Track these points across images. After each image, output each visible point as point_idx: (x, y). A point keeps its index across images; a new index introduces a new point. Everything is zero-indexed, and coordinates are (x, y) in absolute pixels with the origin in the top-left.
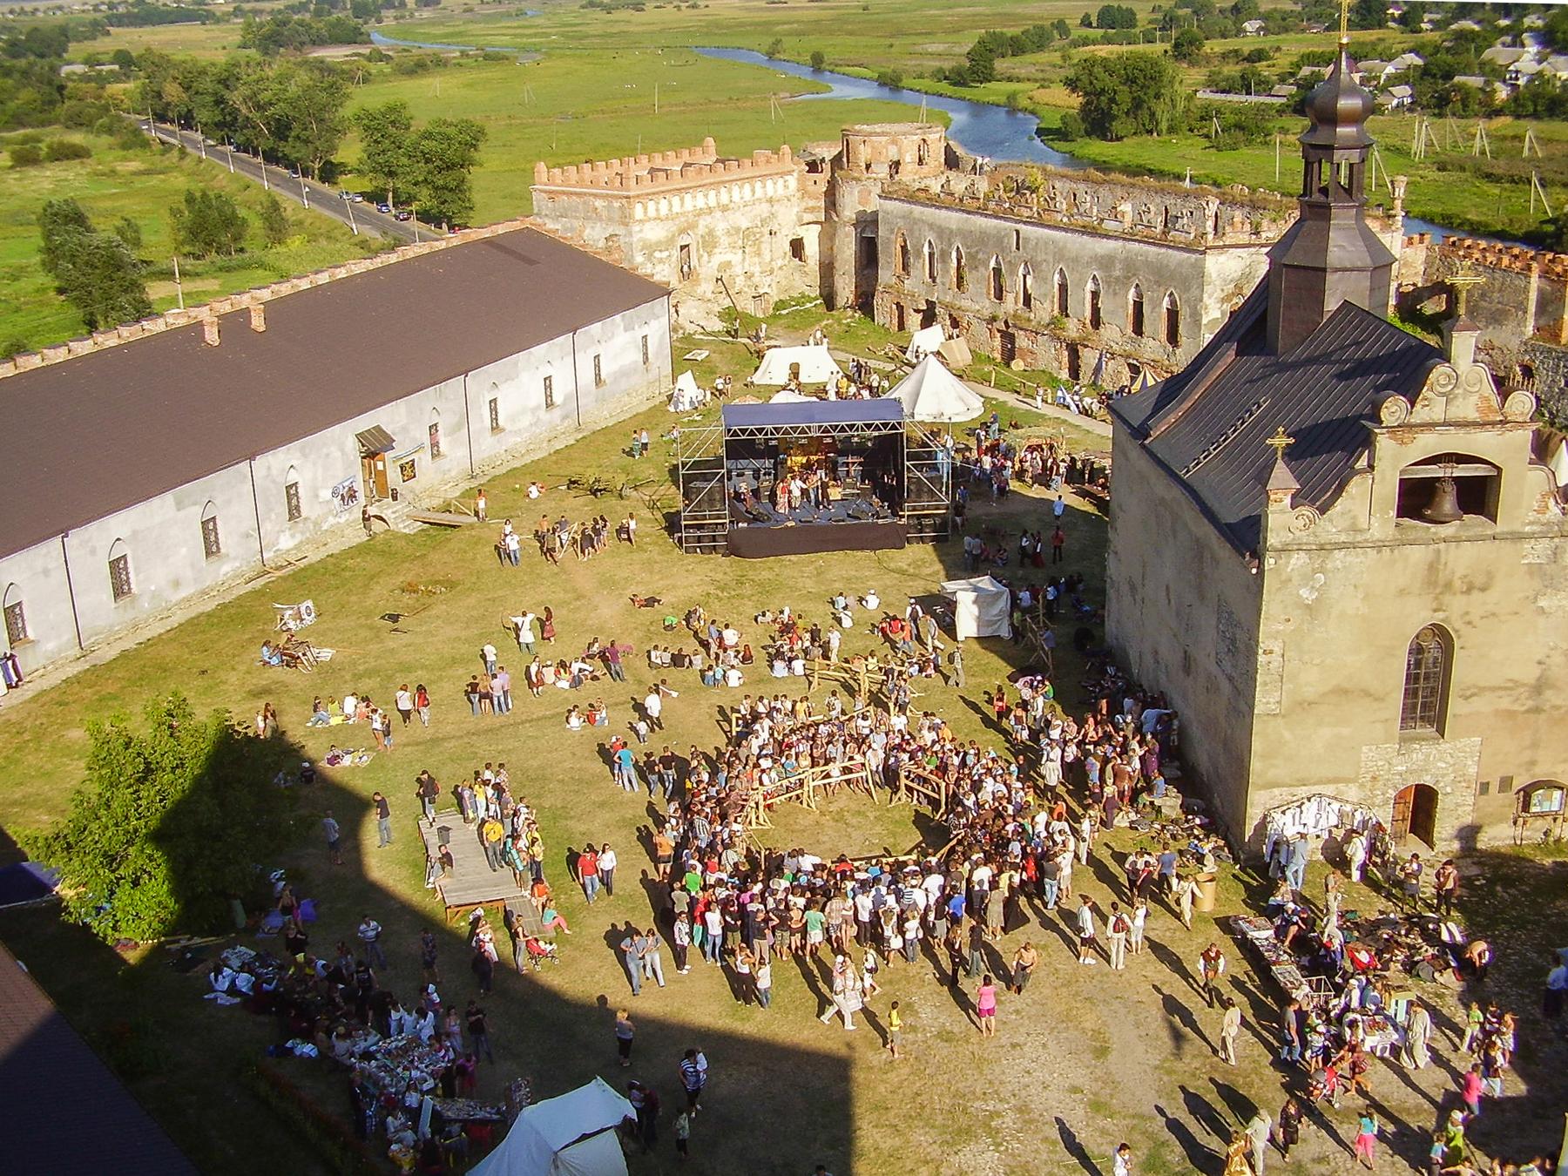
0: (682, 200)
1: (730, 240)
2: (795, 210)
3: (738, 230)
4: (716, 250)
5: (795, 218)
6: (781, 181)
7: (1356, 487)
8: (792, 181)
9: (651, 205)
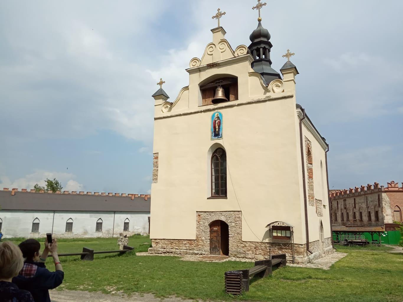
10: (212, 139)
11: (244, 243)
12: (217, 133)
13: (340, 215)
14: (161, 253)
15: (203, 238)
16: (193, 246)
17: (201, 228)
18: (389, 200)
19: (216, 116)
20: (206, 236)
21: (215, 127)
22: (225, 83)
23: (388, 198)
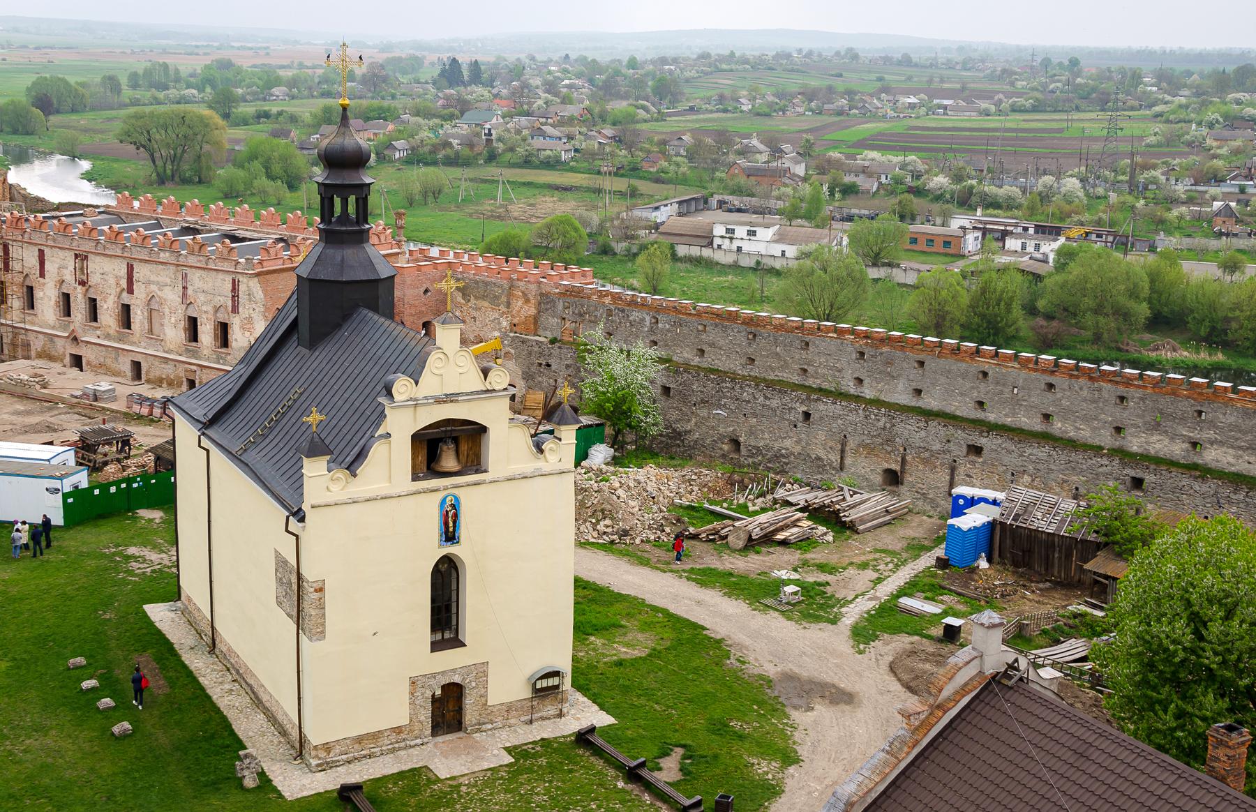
7: (377, 451)
10: (440, 546)
12: (450, 536)
13: (54, 299)
15: (423, 718)
16: (403, 736)
18: (262, 296)
19: (448, 503)
20: (425, 715)
21: (446, 524)
23: (260, 292)
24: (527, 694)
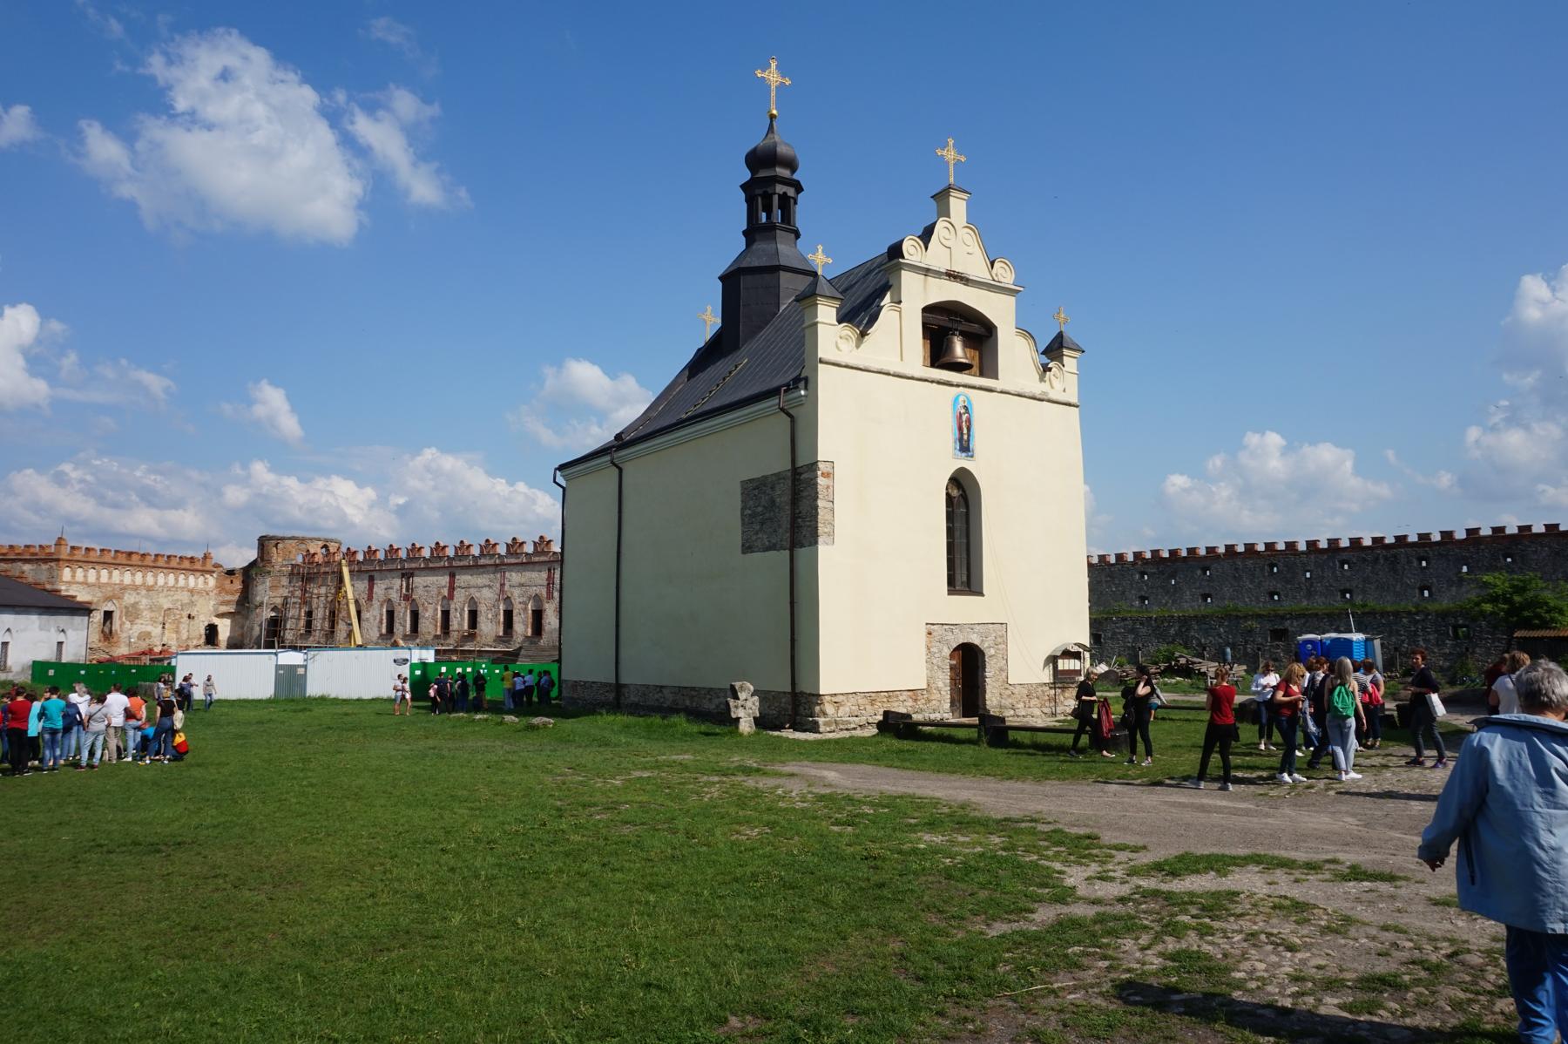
0: (110, 573)
1: (153, 615)
2: (212, 603)
3: (160, 608)
4: (137, 621)
5: (212, 609)
6: (201, 579)
8: (212, 581)
9: (80, 573)
11: (1011, 688)
12: (965, 447)
14: (854, 729)
15: (940, 684)
17: (935, 661)
19: (962, 404)
21: (960, 429)
22: (975, 328)
24: (1046, 676)
